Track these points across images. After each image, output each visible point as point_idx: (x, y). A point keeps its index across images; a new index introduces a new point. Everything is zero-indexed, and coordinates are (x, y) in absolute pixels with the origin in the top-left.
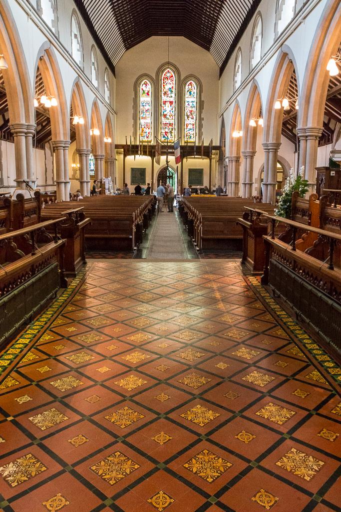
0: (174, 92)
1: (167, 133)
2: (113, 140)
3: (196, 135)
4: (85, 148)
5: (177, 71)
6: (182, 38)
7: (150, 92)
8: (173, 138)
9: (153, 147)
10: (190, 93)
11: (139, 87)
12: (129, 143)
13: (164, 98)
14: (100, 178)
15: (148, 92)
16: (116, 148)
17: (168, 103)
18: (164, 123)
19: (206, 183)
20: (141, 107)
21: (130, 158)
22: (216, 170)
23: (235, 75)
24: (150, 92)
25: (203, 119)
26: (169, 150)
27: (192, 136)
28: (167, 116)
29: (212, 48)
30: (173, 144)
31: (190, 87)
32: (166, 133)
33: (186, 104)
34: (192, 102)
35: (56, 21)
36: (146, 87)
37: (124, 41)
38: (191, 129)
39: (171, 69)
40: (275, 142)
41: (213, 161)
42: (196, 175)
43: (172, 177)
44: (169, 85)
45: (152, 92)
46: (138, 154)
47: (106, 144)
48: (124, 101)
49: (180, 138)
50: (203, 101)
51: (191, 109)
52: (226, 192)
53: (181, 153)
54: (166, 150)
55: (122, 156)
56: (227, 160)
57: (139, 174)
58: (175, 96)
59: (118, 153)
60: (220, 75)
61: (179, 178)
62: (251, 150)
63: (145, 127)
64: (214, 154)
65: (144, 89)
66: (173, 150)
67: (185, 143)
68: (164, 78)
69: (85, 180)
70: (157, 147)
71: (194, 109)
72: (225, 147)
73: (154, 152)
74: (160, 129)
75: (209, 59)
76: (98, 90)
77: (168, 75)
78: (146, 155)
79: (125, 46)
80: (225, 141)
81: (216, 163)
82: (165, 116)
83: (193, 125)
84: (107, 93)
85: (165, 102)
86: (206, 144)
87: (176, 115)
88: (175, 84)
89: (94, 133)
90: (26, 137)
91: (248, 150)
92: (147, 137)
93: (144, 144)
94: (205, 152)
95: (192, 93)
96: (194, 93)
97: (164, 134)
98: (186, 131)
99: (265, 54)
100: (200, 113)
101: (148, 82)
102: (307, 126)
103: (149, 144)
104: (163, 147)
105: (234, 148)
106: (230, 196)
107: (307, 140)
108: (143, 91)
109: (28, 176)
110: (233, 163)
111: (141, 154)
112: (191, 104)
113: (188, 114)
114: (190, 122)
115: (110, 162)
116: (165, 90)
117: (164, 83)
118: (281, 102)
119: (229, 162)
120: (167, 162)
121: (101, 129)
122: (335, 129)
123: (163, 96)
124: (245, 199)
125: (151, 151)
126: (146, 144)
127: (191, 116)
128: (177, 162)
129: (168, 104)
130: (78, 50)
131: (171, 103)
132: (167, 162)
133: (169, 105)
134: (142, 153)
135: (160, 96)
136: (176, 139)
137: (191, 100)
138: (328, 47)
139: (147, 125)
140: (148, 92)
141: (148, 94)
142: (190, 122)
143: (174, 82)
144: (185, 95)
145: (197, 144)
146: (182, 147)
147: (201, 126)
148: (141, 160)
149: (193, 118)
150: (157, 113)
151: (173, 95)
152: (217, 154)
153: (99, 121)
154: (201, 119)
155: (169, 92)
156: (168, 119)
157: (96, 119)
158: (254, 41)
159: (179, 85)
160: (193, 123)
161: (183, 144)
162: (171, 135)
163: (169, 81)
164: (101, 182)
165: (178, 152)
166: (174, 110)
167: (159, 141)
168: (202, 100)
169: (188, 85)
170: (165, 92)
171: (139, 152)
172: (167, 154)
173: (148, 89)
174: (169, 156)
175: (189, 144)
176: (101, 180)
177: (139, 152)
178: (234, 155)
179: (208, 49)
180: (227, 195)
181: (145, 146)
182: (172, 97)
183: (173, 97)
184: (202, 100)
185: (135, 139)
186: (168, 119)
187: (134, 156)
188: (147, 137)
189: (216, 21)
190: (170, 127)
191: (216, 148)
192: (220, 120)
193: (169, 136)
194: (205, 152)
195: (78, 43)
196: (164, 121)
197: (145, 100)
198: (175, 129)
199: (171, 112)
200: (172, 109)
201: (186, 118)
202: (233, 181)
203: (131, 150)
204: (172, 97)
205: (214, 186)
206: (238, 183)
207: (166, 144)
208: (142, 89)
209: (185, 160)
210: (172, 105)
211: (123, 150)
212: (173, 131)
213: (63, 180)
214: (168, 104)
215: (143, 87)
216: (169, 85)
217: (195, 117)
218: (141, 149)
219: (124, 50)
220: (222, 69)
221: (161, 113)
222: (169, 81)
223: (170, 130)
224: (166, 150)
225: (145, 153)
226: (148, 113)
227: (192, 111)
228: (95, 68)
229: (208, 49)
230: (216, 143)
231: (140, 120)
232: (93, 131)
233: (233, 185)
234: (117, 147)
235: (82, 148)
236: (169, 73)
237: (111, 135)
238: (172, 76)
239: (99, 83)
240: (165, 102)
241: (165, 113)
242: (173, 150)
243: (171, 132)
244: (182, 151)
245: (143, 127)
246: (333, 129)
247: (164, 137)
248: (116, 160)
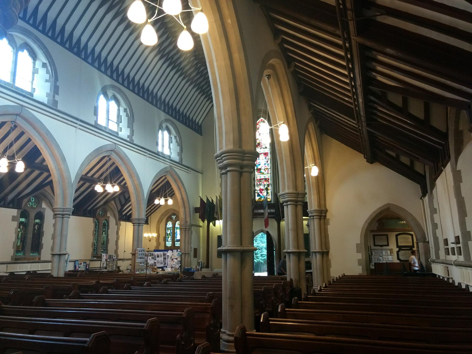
1: (263, 190)
17: (262, 155)
18: (258, 178)
28: (262, 171)
32: (261, 190)
82: (259, 170)
97: (259, 192)
131: (266, 154)
133: (264, 157)
156: (263, 174)
182: (266, 148)
186: (263, 174)
190: (266, 183)
199: (266, 165)
200: (267, 162)
206: (327, 253)
210: (267, 157)
212: (270, 188)
223: (266, 187)
233: (318, 256)
241: (259, 167)
243: (267, 189)
247: (259, 195)
248: (201, 226)
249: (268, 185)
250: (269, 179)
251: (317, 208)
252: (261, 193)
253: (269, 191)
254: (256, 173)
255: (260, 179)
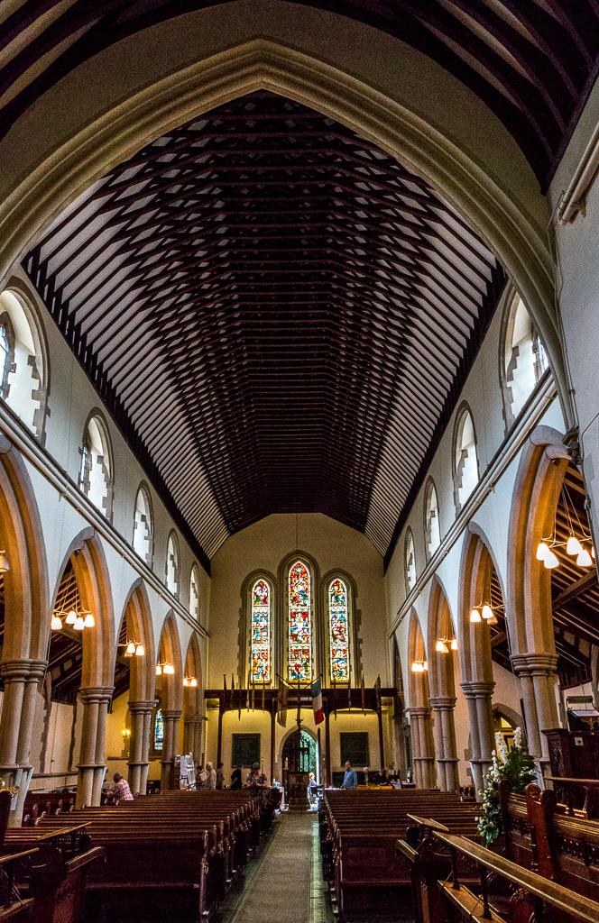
0: (309, 597)
1: (299, 666)
2: (200, 682)
3: (350, 670)
4: (143, 699)
5: (313, 563)
6: (321, 514)
7: (269, 598)
8: (309, 676)
9: (274, 693)
10: (336, 598)
11: (251, 590)
12: (229, 687)
13: (293, 607)
14: (170, 754)
15: (266, 598)
16: (205, 697)
17: (300, 615)
18: (294, 648)
19: (374, 763)
20: (254, 624)
21: (231, 715)
22: (391, 733)
23: (407, 569)
24: (269, 598)
25: (361, 641)
26: (303, 699)
27: (344, 670)
29: (368, 528)
30: (309, 687)
31: (336, 588)
32: (297, 666)
33: (331, 616)
34: (340, 612)
35: (110, 499)
36: (262, 590)
37: (226, 523)
38: (341, 659)
39: (303, 561)
40: (482, 680)
41: (386, 717)
42: (355, 745)
43: (308, 749)
44: (301, 583)
45: (271, 599)
46: (245, 707)
47: (187, 690)
48: (223, 619)
49: (321, 675)
50: (360, 611)
51: (339, 625)
52: (411, 779)
53: (324, 702)
54: (296, 699)
55: (217, 712)
56: (408, 715)
57: (247, 746)
58: (312, 603)
59: (211, 706)
60: (385, 572)
61: (324, 752)
62: (446, 697)
63: (259, 658)
64: (385, 704)
65: (259, 593)
66: (311, 699)
67: (331, 684)
68: (292, 574)
69: (139, 760)
70: (280, 694)
71: (345, 625)
72: (402, 690)
73: (276, 703)
74: (285, 660)
75: (368, 545)
76: (177, 599)
77: (299, 570)
78: (261, 709)
79: (228, 528)
80: (402, 680)
81: (390, 720)
82: (295, 637)
83: (345, 651)
84: (194, 603)
85: (294, 615)
86: (369, 685)
87: (314, 634)
88: (311, 584)
89: (165, 671)
90: (27, 685)
91: (441, 696)
92: (263, 676)
93: (257, 687)
94: (366, 699)
95: (340, 597)
96: (343, 598)
97: (294, 668)
98: (333, 664)
99: (446, 536)
100: (356, 630)
101: (266, 583)
102: (527, 652)
103: (267, 687)
104: (292, 693)
105: (417, 691)
106: (419, 787)
107: (531, 677)
108: (257, 596)
109: (19, 759)
110: (420, 720)
111: (250, 707)
112: (339, 616)
113: (335, 633)
114: (340, 648)
115: (194, 724)
116: (294, 595)
117: (291, 583)
118: (480, 611)
119: (412, 719)
120: (299, 721)
121: (177, 664)
122: (590, 655)
123: (290, 604)
124: (446, 793)
125: (270, 701)
126: (261, 687)
127: (339, 637)
128: (318, 720)
129: (299, 617)
130: (146, 538)
131: (305, 615)
132: (299, 721)
133: (302, 620)
134: (253, 705)
135: (285, 604)
136: (315, 677)
137: (339, 610)
138: (535, 525)
139: (263, 654)
140: (266, 598)
141: (265, 601)
142: (340, 648)
143: (309, 581)
144: (328, 602)
145: (353, 686)
146: (325, 692)
147: (358, 654)
148: (251, 718)
149: (343, 640)
150: (281, 633)
151: (308, 602)
152: (390, 704)
153: (176, 650)
154: (357, 642)
155: (301, 597)
157: (171, 647)
158: (428, 518)
159: (316, 587)
160: (344, 648)
161: (328, 687)
162: (306, 671)
163: (301, 580)
164: (172, 764)
165: (319, 701)
166: (310, 626)
167: (285, 683)
168: (358, 608)
169: (333, 586)
170: (294, 598)
171: (248, 704)
172: (299, 705)
173: (265, 593)
174: (242, 710)
175: (337, 687)
176: (173, 760)
177: (248, 704)
178: (420, 704)
179: (362, 530)
180: (414, 786)
181: (258, 693)
182: (305, 605)
183: (308, 605)
184: (358, 608)
185: (241, 678)
187: (236, 712)
188: (262, 673)
189: (370, 491)
191: (387, 692)
192: (391, 643)
193: (303, 672)
194: (366, 699)
195: (147, 528)
196: (293, 645)
197: (261, 611)
198: (312, 660)
199: (305, 630)
201: (332, 640)
202: (423, 756)
203: (233, 699)
204: (305, 605)
205: (391, 768)
207: (296, 686)
208: (255, 593)
209: (332, 716)
211: (218, 700)
213: (93, 764)
214: (299, 617)
215: (256, 590)
216: (301, 583)
217: (347, 638)
218: (250, 697)
219: (225, 535)
220: (387, 560)
221: (288, 632)
222: (301, 580)
224: (296, 697)
225: (258, 706)
226: (264, 634)
227: (341, 628)
228: (174, 563)
229: (362, 530)
230: (387, 682)
231: (250, 644)
232: (162, 667)
233: (423, 764)
234: (209, 694)
235: (138, 700)
236: (299, 567)
237: (197, 675)
238: (306, 572)
239: (178, 586)
240: (294, 615)
241: (296, 632)
242: (311, 699)
243: (305, 665)
244: (326, 699)
245: (256, 657)
246: (588, 656)
247: (293, 674)
248: (206, 719)
249: (308, 660)
250: (308, 650)
251: (422, 706)
252: (297, 670)
253: (309, 669)
254: (291, 641)
255: (296, 650)
